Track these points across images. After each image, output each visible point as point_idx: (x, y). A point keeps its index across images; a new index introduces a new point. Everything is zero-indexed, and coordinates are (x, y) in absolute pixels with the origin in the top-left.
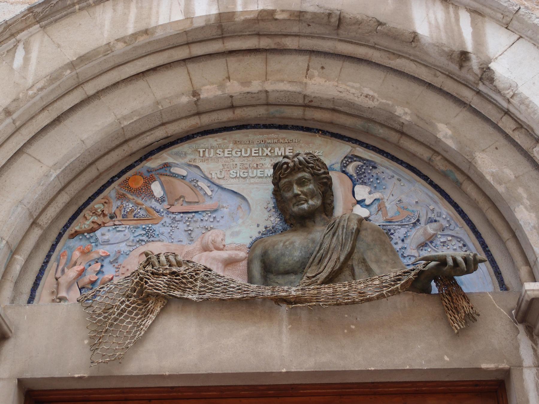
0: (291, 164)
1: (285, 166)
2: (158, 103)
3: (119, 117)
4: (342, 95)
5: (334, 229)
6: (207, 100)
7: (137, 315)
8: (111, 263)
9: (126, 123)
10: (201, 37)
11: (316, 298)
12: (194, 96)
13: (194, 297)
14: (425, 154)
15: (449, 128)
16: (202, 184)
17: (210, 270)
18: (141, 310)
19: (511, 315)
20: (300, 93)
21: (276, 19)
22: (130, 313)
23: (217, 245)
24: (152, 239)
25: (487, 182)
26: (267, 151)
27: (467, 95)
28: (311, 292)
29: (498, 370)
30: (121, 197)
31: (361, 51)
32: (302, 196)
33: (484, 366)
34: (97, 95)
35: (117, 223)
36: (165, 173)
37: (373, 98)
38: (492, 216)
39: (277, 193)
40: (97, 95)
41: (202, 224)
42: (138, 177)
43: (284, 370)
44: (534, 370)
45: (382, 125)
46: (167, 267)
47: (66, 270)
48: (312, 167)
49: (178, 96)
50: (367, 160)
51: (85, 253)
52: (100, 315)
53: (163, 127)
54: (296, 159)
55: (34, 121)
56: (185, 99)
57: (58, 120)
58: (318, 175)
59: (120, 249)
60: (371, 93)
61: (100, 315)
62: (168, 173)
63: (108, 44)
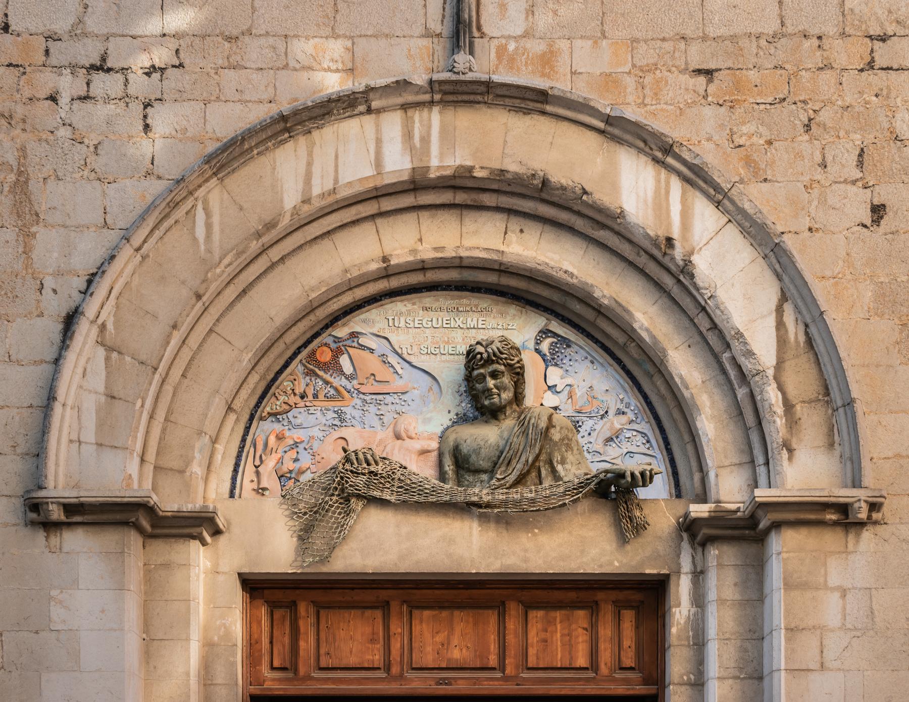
0: (485, 356)
1: (479, 356)
2: (346, 271)
3: (306, 288)
4: (539, 267)
5: (523, 423)
6: (398, 265)
7: (340, 514)
8: (305, 449)
9: (313, 295)
10: (391, 191)
11: (505, 503)
12: (384, 262)
13: (393, 498)
14: (621, 339)
15: (646, 315)
16: (393, 359)
17: (405, 468)
18: (343, 508)
19: (678, 523)
20: (496, 261)
21: (475, 177)
22: (334, 513)
23: (410, 434)
24: (345, 424)
25: (675, 383)
26: (459, 322)
27: (668, 281)
28: (501, 497)
29: (659, 575)
30: (310, 373)
31: (563, 216)
32: (495, 390)
33: (647, 571)
34: (282, 259)
35: (308, 404)
36: (353, 344)
37: (572, 275)
38: (677, 415)
39: (469, 379)
40: (282, 259)
41: (393, 407)
42: (325, 348)
43: (474, 571)
44: (690, 576)
45: (580, 300)
46: (365, 465)
47: (264, 457)
48: (506, 359)
49: (367, 263)
50: (562, 337)
51: (280, 438)
52: (305, 514)
53: (350, 292)
54: (490, 350)
55: (221, 297)
56: (374, 266)
57: (245, 291)
58: (511, 366)
59: (316, 436)
60: (570, 269)
61: (305, 514)
62: (356, 345)
63: (295, 207)
